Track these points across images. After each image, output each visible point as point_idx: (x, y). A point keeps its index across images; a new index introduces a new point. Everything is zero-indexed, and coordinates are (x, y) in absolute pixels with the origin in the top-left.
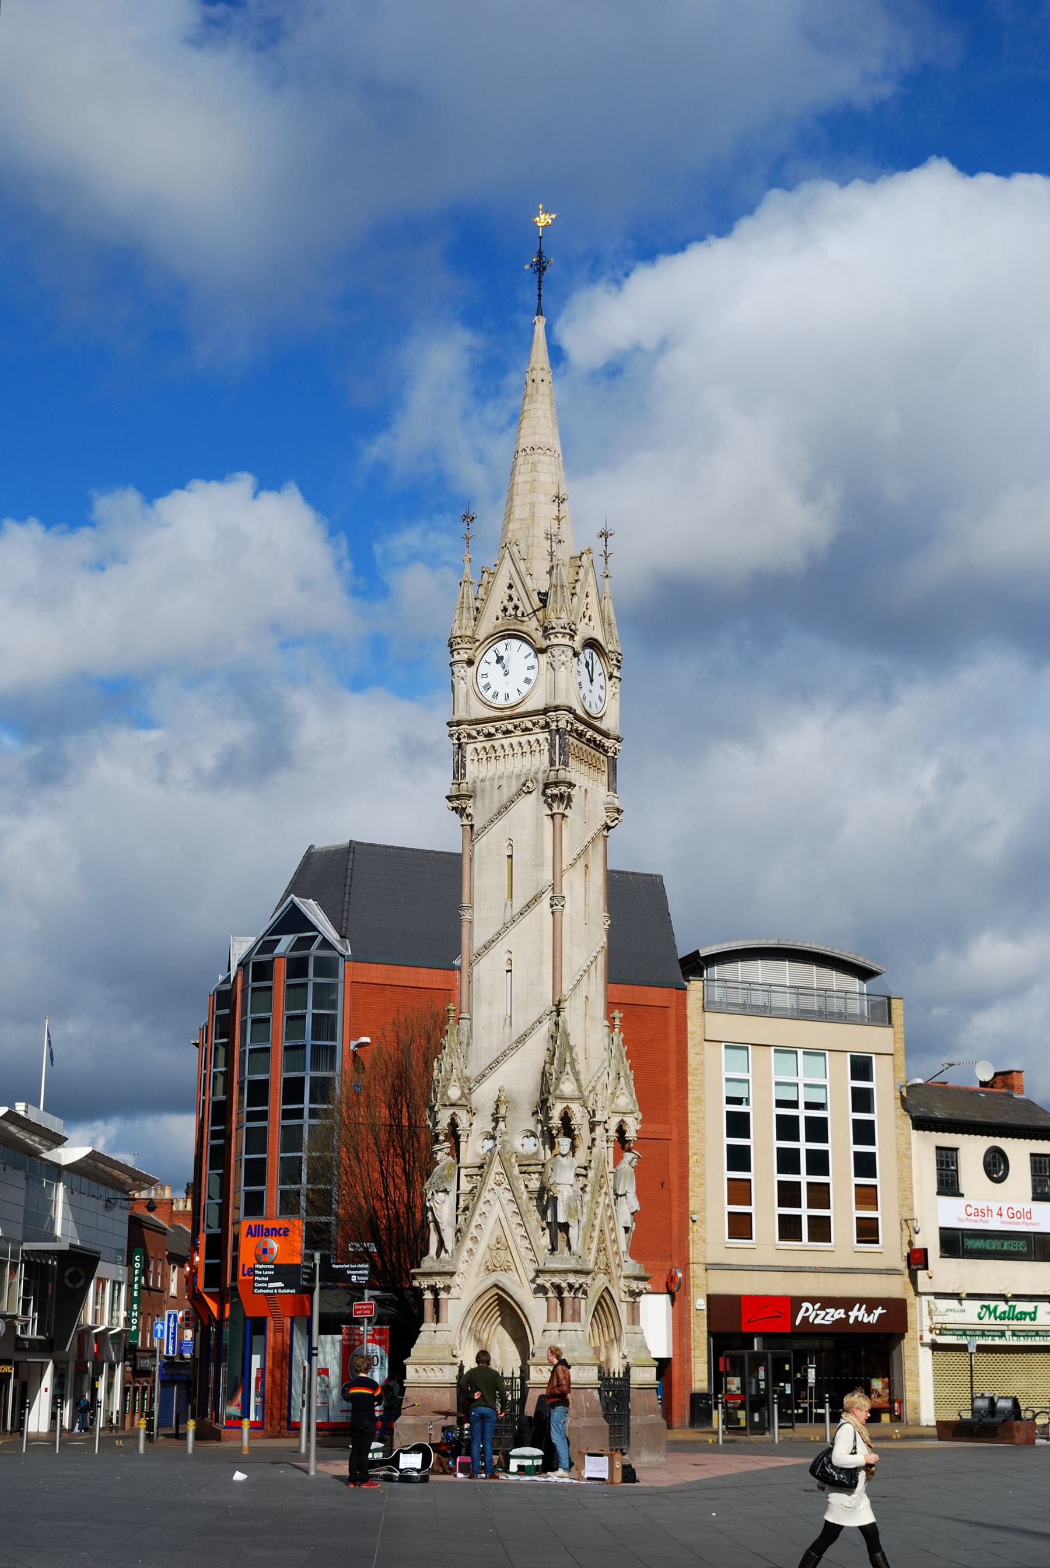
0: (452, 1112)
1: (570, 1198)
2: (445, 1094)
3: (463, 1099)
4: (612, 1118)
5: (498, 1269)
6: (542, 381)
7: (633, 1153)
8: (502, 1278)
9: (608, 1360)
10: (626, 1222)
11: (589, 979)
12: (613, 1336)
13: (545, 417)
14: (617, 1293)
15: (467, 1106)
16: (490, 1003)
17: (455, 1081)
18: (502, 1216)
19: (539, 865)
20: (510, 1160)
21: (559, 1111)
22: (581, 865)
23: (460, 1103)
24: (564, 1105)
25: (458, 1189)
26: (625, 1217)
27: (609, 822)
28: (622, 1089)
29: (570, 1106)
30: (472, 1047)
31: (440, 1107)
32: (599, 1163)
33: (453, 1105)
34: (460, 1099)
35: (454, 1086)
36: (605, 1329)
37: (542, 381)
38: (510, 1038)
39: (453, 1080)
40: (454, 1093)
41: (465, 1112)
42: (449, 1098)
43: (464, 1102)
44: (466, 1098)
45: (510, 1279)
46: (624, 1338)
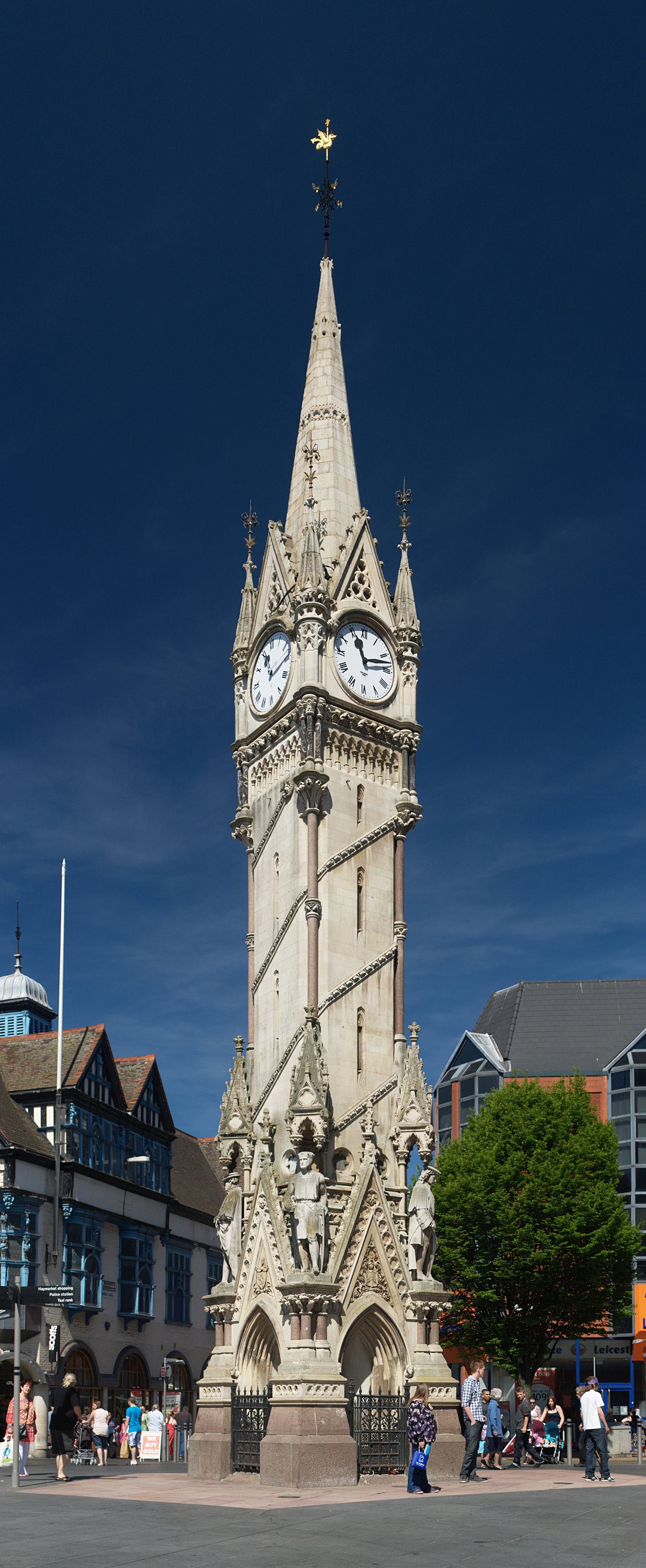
0: (232, 1141)
1: (310, 1213)
2: (225, 1125)
3: (245, 1128)
4: (402, 1134)
5: (262, 1291)
6: (324, 334)
7: (429, 1169)
8: (263, 1300)
9: (392, 1378)
10: (415, 1240)
11: (365, 989)
12: (395, 1355)
13: (325, 374)
14: (400, 1311)
15: (246, 1134)
16: (265, 1028)
17: (236, 1111)
18: (264, 1239)
19: (295, 873)
20: (269, 1182)
21: (298, 1124)
22: (348, 869)
23: (240, 1131)
24: (304, 1118)
25: (243, 1217)
26: (416, 1235)
27: (400, 821)
28: (412, 1103)
29: (311, 1118)
30: (254, 1075)
31: (221, 1138)
32: (365, 1178)
33: (232, 1135)
34: (242, 1127)
35: (235, 1116)
36: (393, 1347)
37: (324, 334)
38: (278, 1059)
39: (233, 1110)
40: (235, 1124)
41: (246, 1141)
42: (229, 1128)
43: (245, 1130)
44: (247, 1127)
45: (269, 1300)
46: (409, 1358)
